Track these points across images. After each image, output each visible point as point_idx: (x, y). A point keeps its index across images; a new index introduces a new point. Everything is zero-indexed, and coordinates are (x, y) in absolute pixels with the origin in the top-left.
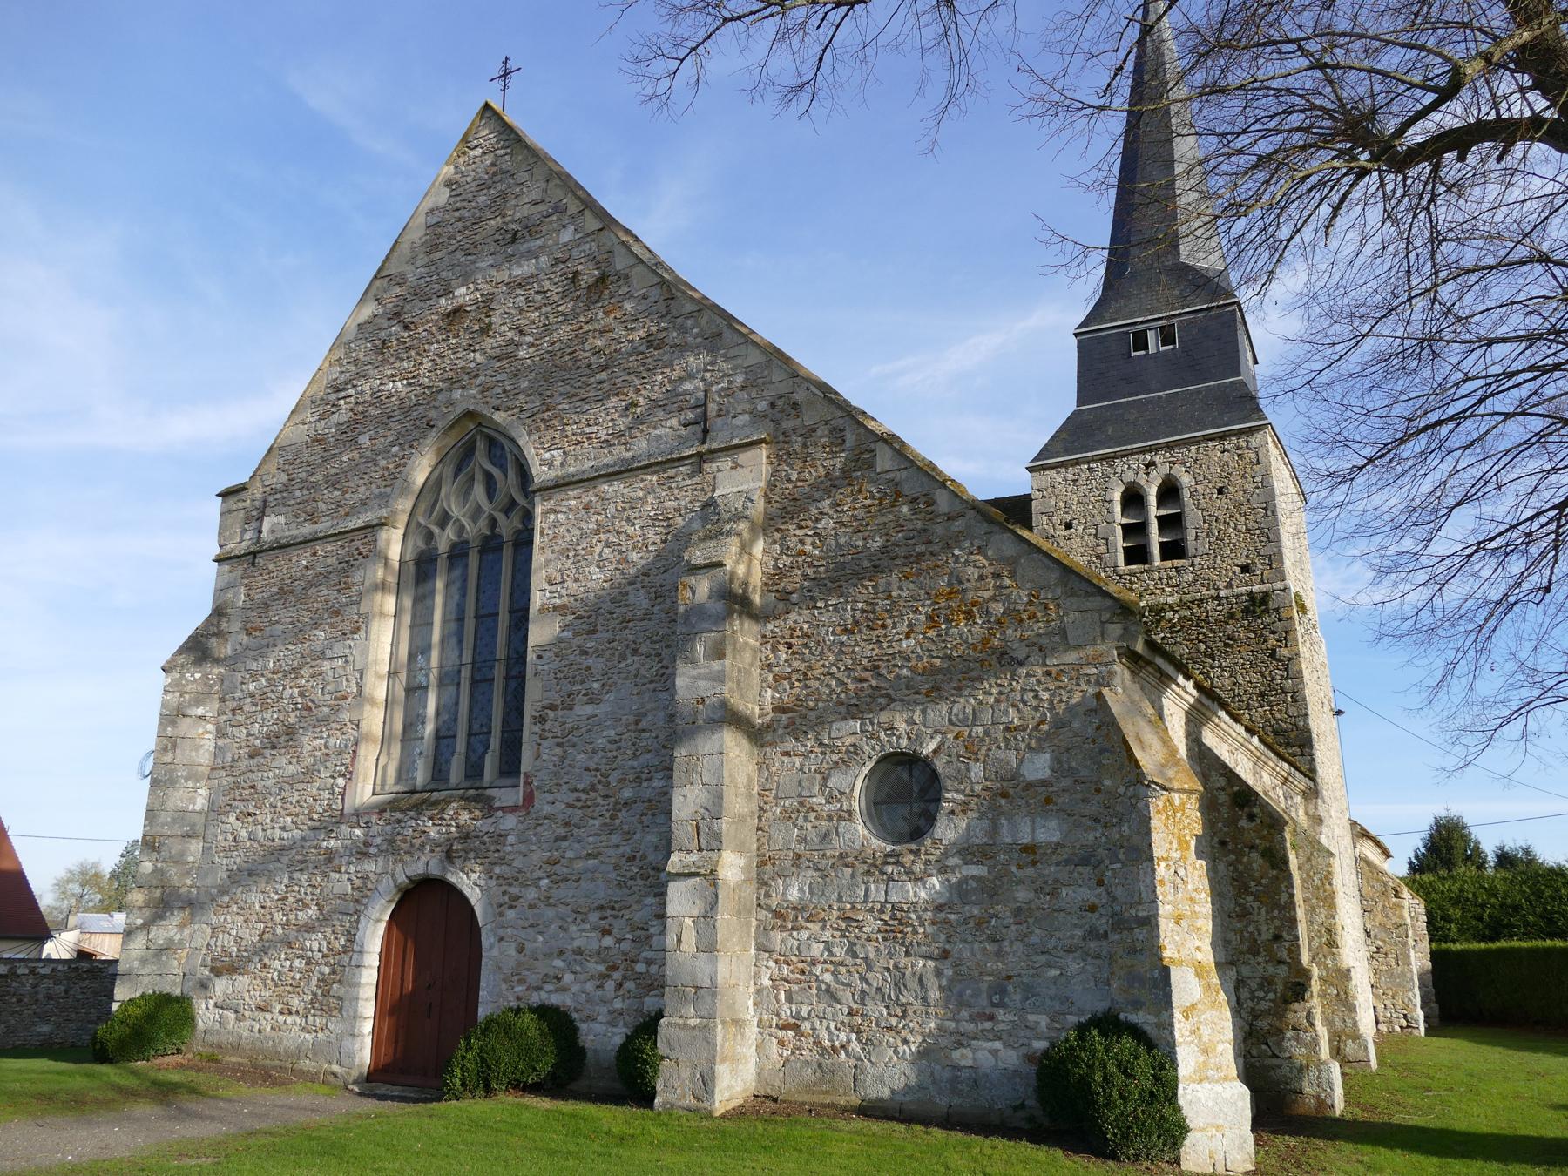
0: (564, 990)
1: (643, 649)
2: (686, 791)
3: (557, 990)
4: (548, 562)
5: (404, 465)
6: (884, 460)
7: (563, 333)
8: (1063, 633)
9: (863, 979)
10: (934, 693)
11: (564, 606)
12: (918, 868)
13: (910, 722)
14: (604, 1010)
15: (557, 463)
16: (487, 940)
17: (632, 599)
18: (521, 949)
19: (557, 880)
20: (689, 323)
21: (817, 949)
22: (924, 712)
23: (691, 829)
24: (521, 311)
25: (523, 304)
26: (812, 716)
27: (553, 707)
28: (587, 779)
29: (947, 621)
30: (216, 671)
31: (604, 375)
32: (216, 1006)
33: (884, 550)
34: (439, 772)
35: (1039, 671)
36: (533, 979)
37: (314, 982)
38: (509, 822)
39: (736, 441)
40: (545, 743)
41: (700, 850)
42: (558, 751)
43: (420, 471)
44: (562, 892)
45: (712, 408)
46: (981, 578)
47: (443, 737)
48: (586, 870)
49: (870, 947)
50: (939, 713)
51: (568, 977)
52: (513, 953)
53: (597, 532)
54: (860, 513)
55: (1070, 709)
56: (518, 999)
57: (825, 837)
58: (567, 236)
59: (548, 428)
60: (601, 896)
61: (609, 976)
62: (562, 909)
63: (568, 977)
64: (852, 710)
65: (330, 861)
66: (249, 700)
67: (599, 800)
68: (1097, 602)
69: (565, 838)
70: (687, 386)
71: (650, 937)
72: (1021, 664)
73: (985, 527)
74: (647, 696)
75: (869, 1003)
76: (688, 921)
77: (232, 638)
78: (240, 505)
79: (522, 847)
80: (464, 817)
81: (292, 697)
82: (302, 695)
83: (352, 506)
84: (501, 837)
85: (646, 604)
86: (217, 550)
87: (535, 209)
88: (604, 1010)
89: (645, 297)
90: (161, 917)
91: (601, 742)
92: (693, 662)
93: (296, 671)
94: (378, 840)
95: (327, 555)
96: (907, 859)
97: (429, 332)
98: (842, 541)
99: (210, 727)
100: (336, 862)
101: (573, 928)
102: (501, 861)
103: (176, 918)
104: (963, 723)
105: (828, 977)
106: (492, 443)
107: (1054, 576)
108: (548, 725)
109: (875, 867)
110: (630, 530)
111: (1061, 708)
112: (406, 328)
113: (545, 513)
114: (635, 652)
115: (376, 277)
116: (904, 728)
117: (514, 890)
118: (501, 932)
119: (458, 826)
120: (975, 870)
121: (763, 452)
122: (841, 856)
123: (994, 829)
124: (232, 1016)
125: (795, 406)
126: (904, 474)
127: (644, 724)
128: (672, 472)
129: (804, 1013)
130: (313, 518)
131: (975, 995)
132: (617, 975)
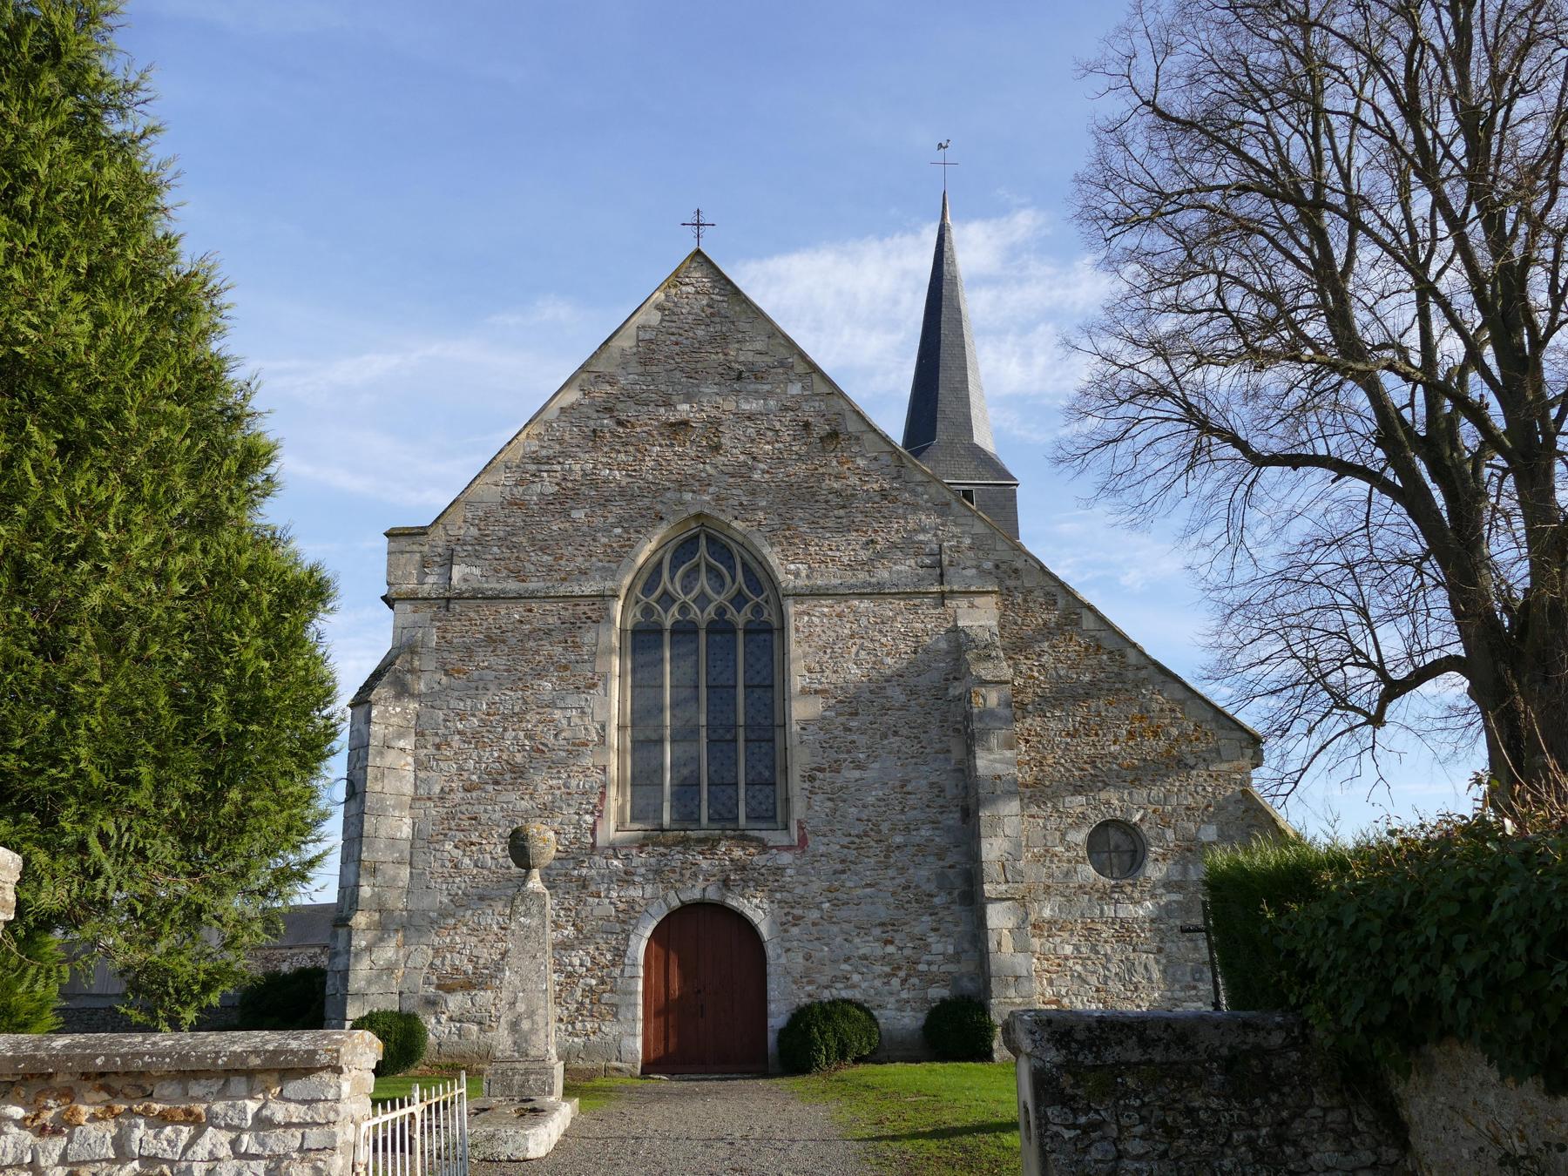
0: (854, 986)
1: (904, 731)
2: (992, 840)
3: (846, 988)
4: (805, 656)
5: (632, 547)
6: (1088, 622)
7: (800, 469)
8: (1218, 751)
9: (1105, 967)
10: (1137, 782)
11: (824, 691)
12: (1136, 895)
13: (1121, 800)
14: (892, 1000)
15: (804, 574)
16: (771, 952)
17: (889, 692)
18: (808, 957)
19: (837, 904)
20: (920, 489)
21: (1068, 950)
22: (1130, 794)
23: (998, 867)
24: (753, 441)
25: (754, 435)
26: (1049, 791)
27: (821, 770)
28: (859, 828)
29: (1142, 736)
30: (413, 706)
31: (842, 512)
32: (451, 1019)
33: (1092, 683)
34: (686, 816)
35: (1205, 774)
36: (824, 980)
37: (579, 993)
38: (786, 858)
39: (973, 588)
40: (817, 798)
41: (1007, 882)
42: (830, 804)
43: (645, 551)
44: (844, 913)
45: (946, 559)
46: (1162, 710)
47: (686, 789)
48: (866, 897)
49: (1108, 947)
50: (1141, 794)
51: (856, 978)
52: (801, 960)
53: (852, 637)
54: (1073, 656)
55: (1226, 799)
56: (810, 996)
57: (1067, 874)
58: (795, 389)
59: (791, 544)
60: (883, 914)
61: (895, 975)
62: (845, 926)
63: (856, 978)
64: (1078, 790)
65: (585, 887)
66: (457, 737)
67: (872, 843)
68: (1238, 734)
69: (843, 872)
70: (921, 537)
71: (928, 945)
72: (1192, 768)
73: (1162, 677)
74: (910, 768)
75: (1110, 983)
76: (1006, 932)
77: (427, 676)
78: (415, 548)
79: (803, 879)
80: (738, 853)
81: (516, 738)
82: (530, 737)
83: (569, 573)
84: (780, 870)
85: (903, 698)
86: (384, 590)
87: (758, 358)
88: (892, 1000)
89: (876, 459)
90: (381, 939)
91: (871, 800)
92: (989, 750)
93: (520, 716)
94: (643, 870)
95: (549, 615)
96: (1128, 889)
97: (649, 434)
98: (1062, 673)
99: (410, 760)
100: (593, 888)
101: (857, 940)
102: (782, 889)
103: (395, 940)
104: (1158, 803)
105: (1079, 968)
106: (711, 540)
107: (1210, 715)
108: (817, 784)
109: (1105, 896)
110: (884, 640)
111: (1220, 798)
112: (620, 423)
113: (800, 614)
114: (896, 733)
115: (583, 368)
116: (1115, 801)
117: (798, 912)
118: (787, 945)
119: (732, 860)
120: (1175, 897)
121: (991, 601)
122: (1080, 887)
123: (1185, 871)
124: (475, 1028)
125: (1016, 571)
126: (1103, 634)
127: (909, 788)
128: (917, 601)
129: (1063, 992)
130: (519, 575)
131: (1183, 974)
132: (902, 974)
